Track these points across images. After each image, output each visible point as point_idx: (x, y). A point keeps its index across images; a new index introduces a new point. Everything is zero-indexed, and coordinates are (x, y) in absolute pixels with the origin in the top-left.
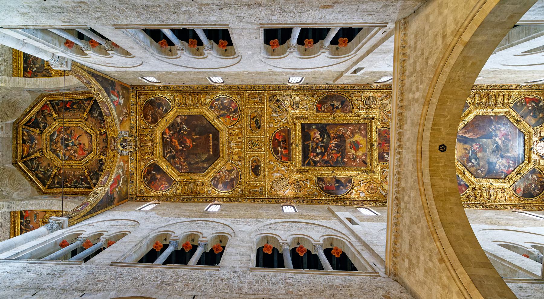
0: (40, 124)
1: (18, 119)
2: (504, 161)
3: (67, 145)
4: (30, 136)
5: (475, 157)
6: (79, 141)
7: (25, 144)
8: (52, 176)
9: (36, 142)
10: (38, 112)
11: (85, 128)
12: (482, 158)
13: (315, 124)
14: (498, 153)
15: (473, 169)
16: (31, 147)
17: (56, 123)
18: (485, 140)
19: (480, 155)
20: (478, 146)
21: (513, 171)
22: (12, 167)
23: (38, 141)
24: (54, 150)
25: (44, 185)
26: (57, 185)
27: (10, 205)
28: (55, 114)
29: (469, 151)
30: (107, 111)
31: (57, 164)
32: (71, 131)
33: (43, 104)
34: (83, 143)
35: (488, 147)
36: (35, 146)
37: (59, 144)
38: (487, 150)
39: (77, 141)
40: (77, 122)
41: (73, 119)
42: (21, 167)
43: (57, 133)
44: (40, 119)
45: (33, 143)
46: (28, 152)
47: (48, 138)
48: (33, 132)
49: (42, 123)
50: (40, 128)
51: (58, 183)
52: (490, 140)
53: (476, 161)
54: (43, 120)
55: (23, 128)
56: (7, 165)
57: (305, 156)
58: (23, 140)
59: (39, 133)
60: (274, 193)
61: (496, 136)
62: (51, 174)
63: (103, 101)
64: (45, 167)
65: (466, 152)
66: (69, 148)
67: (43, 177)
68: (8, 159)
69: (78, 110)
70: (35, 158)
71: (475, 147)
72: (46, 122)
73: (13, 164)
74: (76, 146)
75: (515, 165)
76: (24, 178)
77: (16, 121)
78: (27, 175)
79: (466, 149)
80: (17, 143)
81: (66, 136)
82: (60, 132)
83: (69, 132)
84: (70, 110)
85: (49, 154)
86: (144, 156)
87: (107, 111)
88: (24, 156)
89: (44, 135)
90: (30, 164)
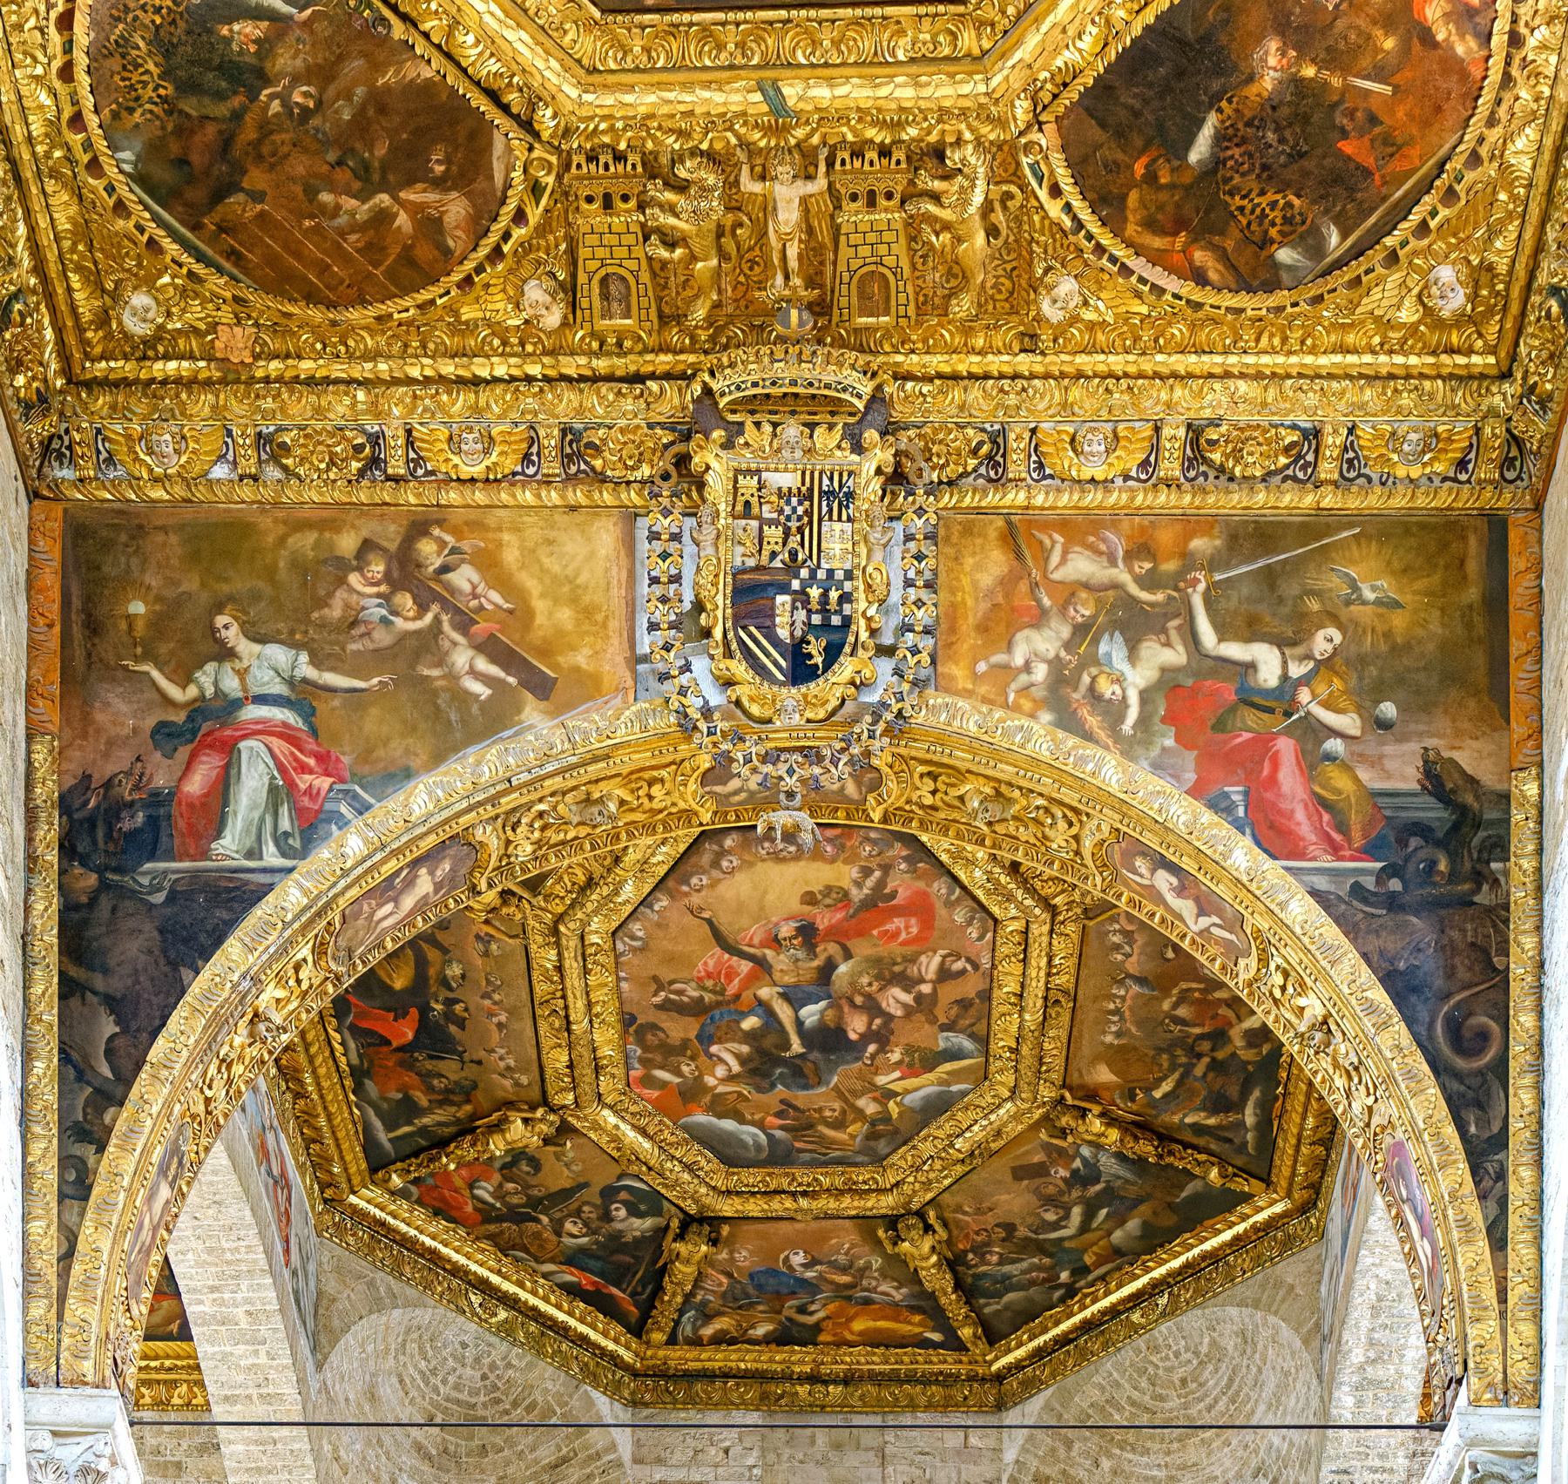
0: (618, 1235)
3: (829, 1040)
4: (736, 1300)
6: (775, 942)
7: (817, 1328)
8: (1146, 1148)
9: (798, 1259)
10: (504, 1247)
11: (630, 892)
16: (843, 1294)
17: (596, 1126)
23: (794, 1245)
24: (872, 1136)
25: (1226, 1203)
26: (1239, 1107)
28: (498, 1127)
31: (1016, 1117)
32: (665, 1006)
34: (795, 906)
36: (833, 1265)
37: (820, 1099)
39: (780, 961)
40: (572, 966)
41: (541, 988)
42: (1039, 1354)
43: (701, 1118)
44: (575, 1234)
45: (804, 1282)
46: (894, 1310)
47: (751, 1177)
48: (700, 1278)
49: (607, 1217)
51: (1219, 1104)
54: (578, 1213)
55: (672, 1341)
58: (782, 1338)
59: (714, 1242)
62: (1120, 1156)
64: (1050, 1201)
66: (856, 1025)
67: (1142, 1208)
69: (432, 954)
70: (953, 1264)
72: (592, 1194)
73: (1000, 1406)
74: (829, 967)
76: (1141, 1343)
78: (1113, 1312)
80: (813, 1379)
81: (728, 1056)
83: (679, 1029)
84: (449, 1016)
86: (957, 274)
88: (936, 1337)
89: (727, 1208)
90: (1010, 1297)
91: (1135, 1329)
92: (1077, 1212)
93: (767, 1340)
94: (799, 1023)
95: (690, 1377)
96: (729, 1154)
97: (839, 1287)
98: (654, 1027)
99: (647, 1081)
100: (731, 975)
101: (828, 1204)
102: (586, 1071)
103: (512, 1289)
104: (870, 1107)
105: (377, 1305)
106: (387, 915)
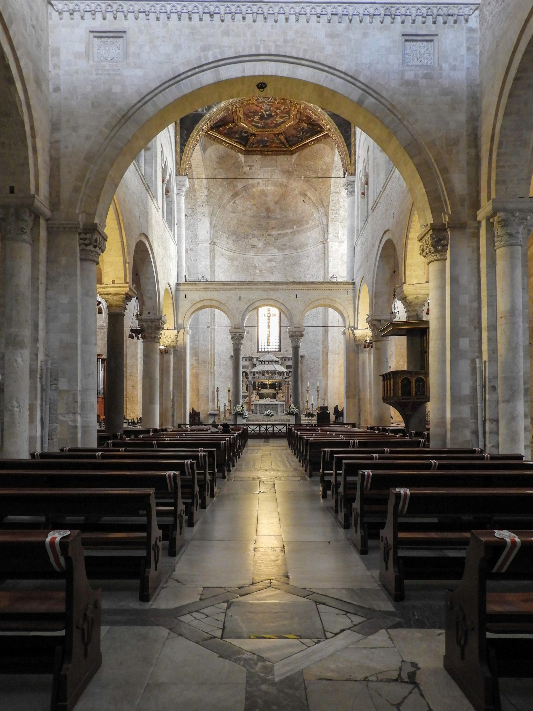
1: (239, 151)
3: (270, 116)
7: (268, 146)
9: (266, 138)
10: (228, 137)
22: (295, 156)
23: (265, 137)
27: (336, 169)
28: (228, 125)
30: (223, 113)
33: (217, 134)
37: (269, 121)
43: (253, 124)
44: (237, 136)
47: (260, 130)
48: (253, 140)
49: (241, 134)
50: (248, 136)
56: (293, 161)
58: (263, 147)
59: (255, 136)
63: (210, 122)
64: (298, 132)
66: (273, 114)
68: (286, 159)
70: (286, 138)
74: (270, 108)
77: (241, 153)
78: (307, 143)
80: (268, 151)
81: (257, 118)
82: (252, 121)
85: (282, 128)
87: (223, 113)
89: (256, 133)
91: (309, 146)
92: (301, 133)
93: (262, 147)
94: (266, 114)
95: (251, 151)
96: (257, 127)
97: (271, 142)
98: (248, 114)
99: (247, 120)
100: (257, 109)
101: (269, 132)
102: (239, 119)
103: (229, 142)
104: (275, 122)
105: (211, 145)
106: (218, 117)
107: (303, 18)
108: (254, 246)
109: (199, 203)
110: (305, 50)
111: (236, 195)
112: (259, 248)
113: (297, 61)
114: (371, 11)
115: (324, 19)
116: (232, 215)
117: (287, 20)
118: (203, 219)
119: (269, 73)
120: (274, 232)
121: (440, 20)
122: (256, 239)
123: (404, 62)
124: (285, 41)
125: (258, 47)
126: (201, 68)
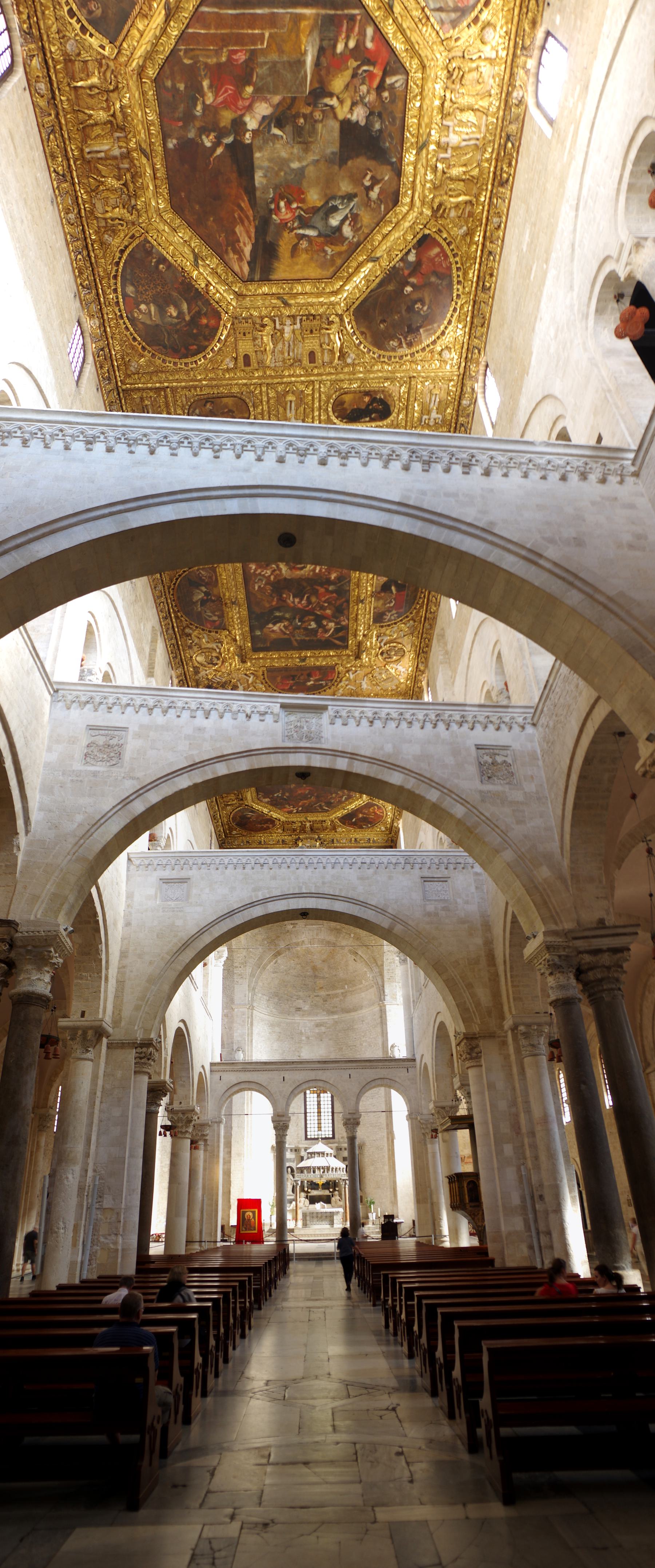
2: (338, 84)
5: (321, 213)
12: (329, 182)
13: (252, 629)
14: (305, 116)
15: (366, 218)
18: (259, 178)
19: (314, 197)
20: (282, 204)
21: (377, 29)
29: (303, 236)
35: (283, 163)
38: (295, 165)
52: (257, 155)
53: (335, 209)
57: (327, 645)
60: (403, 686)
61: (238, 125)
65: (306, 250)
71: (284, 214)
75: (352, 18)
79: (295, 250)
107: (338, 867)
108: (299, 1009)
109: (236, 965)
110: (340, 890)
111: (278, 954)
112: (305, 1011)
113: (334, 897)
114: (394, 861)
115: (356, 867)
116: (273, 975)
117: (324, 868)
118: (240, 981)
119: (311, 907)
120: (323, 993)
121: (451, 867)
122: (301, 1001)
123: (425, 898)
124: (324, 883)
125: (300, 888)
126: (252, 905)
